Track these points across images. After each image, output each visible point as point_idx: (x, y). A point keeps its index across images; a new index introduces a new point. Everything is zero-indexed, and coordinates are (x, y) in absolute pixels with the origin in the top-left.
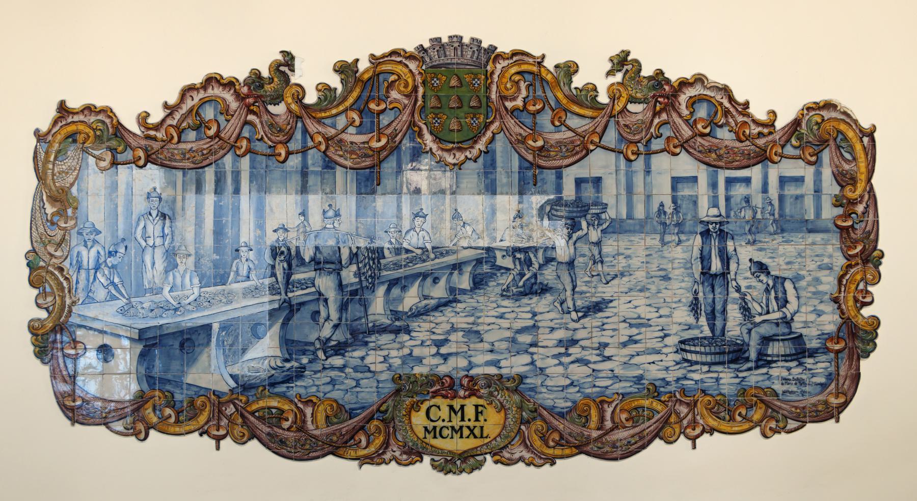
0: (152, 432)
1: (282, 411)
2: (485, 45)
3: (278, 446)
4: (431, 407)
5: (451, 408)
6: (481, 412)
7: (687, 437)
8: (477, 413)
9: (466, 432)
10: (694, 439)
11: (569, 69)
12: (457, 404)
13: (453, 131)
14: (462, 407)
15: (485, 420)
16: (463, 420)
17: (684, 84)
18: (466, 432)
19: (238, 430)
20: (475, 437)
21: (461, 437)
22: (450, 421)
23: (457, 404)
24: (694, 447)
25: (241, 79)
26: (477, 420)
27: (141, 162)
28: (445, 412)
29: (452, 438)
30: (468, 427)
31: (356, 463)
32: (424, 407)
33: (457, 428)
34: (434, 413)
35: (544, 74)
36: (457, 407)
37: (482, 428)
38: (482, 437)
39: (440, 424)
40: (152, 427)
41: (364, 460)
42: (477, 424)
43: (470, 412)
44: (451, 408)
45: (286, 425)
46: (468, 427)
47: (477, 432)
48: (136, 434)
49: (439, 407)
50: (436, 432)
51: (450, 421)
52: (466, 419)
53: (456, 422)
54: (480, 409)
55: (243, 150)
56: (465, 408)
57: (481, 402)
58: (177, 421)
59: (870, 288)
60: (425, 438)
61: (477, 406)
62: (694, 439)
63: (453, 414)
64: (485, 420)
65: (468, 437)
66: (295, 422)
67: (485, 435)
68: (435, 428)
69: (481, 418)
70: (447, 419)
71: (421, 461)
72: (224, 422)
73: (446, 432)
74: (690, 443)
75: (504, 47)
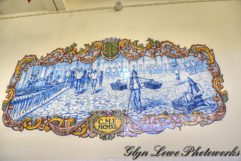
0: (24, 129)
1: (59, 122)
2: (118, 38)
3: (57, 132)
4: (100, 120)
5: (106, 120)
6: (115, 121)
7: (178, 127)
8: (114, 121)
9: (111, 127)
10: (180, 127)
11: (137, 42)
12: (108, 119)
13: (110, 54)
14: (110, 120)
15: (116, 123)
16: (110, 123)
17: (162, 42)
18: (111, 127)
19: (47, 128)
20: (113, 128)
21: (109, 128)
22: (106, 124)
23: (108, 118)
24: (180, 130)
25: (64, 49)
26: (114, 123)
27: (39, 65)
28: (104, 121)
29: (107, 129)
30: (111, 125)
31: (78, 136)
32: (98, 120)
33: (108, 126)
34: (101, 122)
35: (131, 42)
36: (108, 120)
37: (115, 125)
38: (115, 128)
39: (103, 125)
40: (24, 128)
41: (80, 136)
42: (113, 124)
43: (112, 121)
44: (106, 120)
45: (59, 126)
46: (111, 125)
47: (114, 127)
48: (20, 130)
49: (102, 120)
50: (102, 127)
51: (106, 124)
52: (111, 123)
53: (108, 124)
54: (115, 120)
55: (62, 61)
56: (111, 120)
57: (115, 118)
58: (31, 126)
59: (221, 83)
60: (99, 129)
61: (113, 119)
62: (180, 127)
63: (107, 122)
64: (116, 123)
65: (111, 128)
66: (62, 125)
67: (116, 128)
68: (102, 126)
69: (115, 122)
70: (105, 123)
71: (97, 136)
72: (44, 125)
73: (105, 127)
74: (178, 128)
75: (122, 38)
